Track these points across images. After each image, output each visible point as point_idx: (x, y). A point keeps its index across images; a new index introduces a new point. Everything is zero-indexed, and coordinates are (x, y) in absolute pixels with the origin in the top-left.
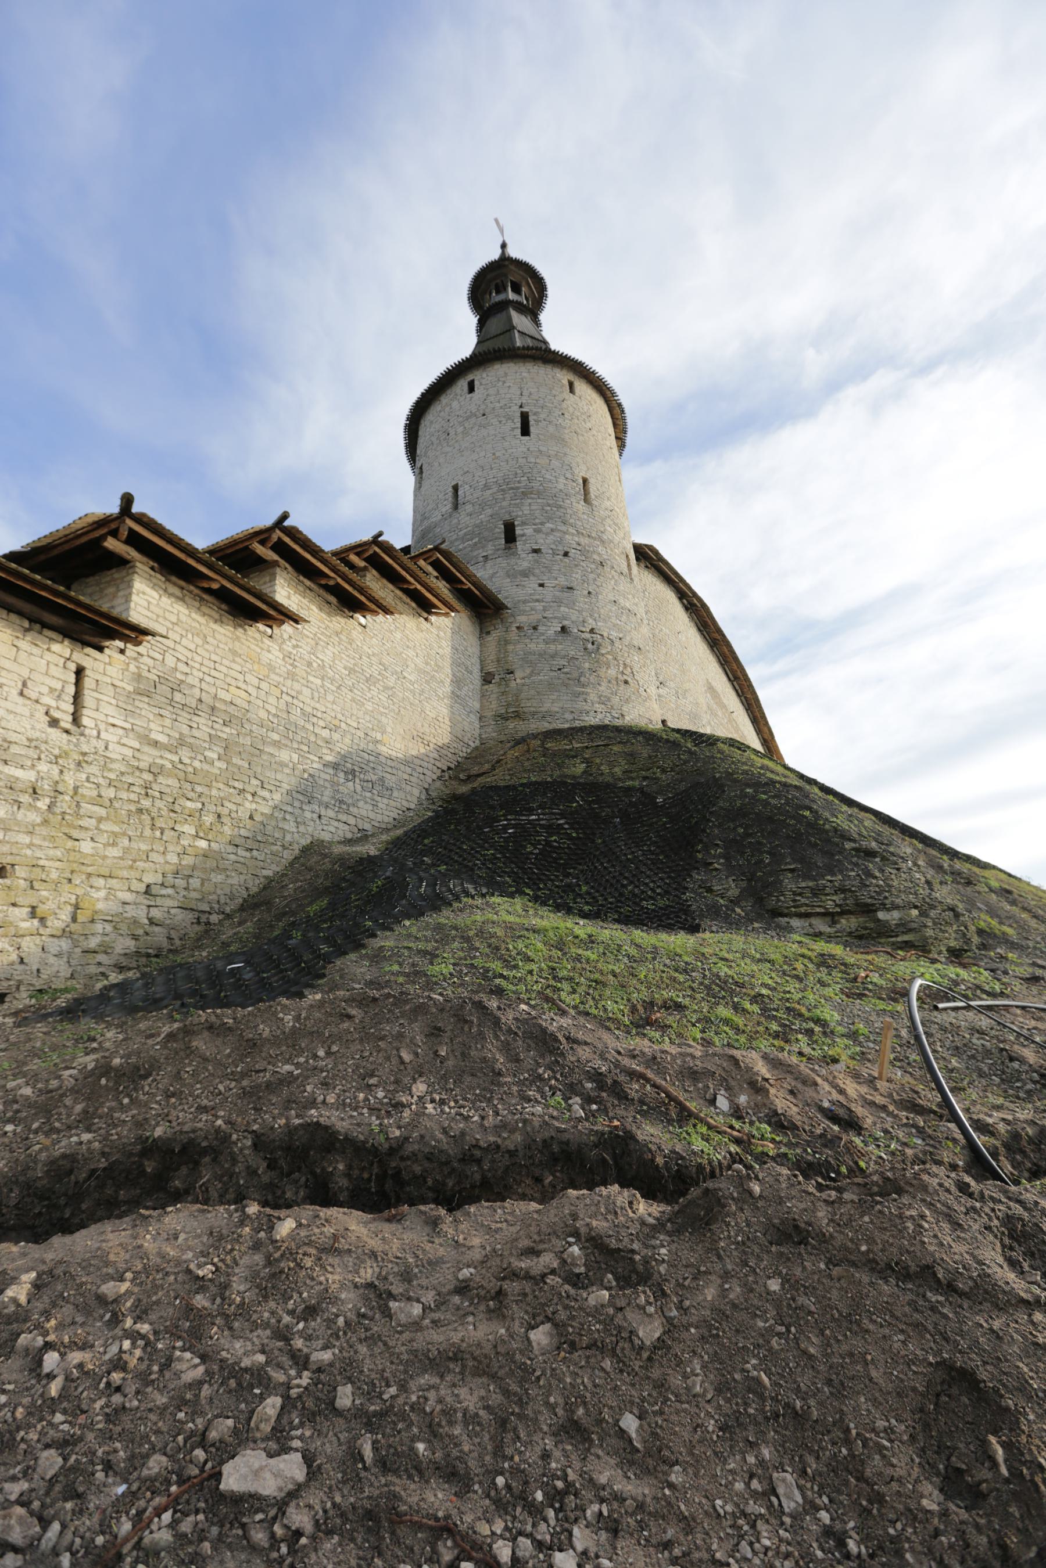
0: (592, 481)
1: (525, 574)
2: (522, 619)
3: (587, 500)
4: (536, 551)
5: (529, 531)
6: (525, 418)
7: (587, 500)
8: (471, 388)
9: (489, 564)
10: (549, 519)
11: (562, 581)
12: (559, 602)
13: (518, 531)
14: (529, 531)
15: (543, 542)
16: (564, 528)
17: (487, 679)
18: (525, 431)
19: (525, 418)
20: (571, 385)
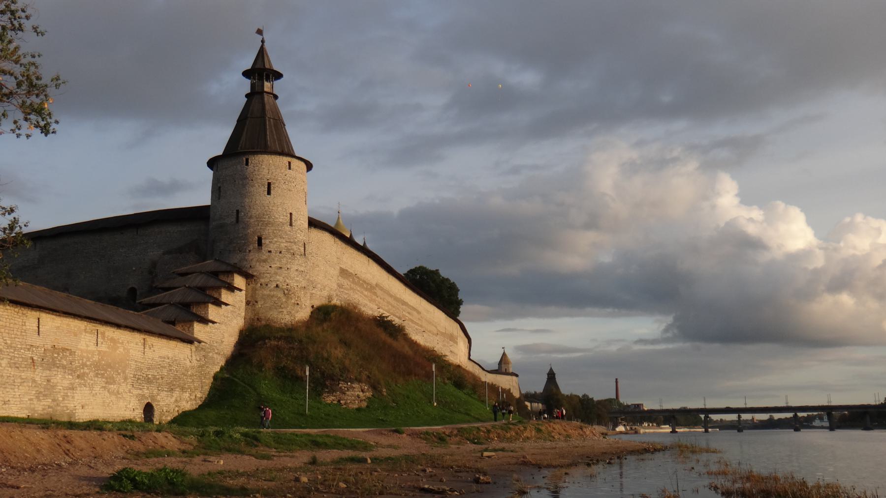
0: (293, 213)
1: (265, 261)
2: (262, 281)
3: (291, 225)
4: (270, 252)
5: (267, 242)
6: (269, 184)
7: (291, 225)
8: (247, 164)
9: (251, 254)
10: (275, 237)
11: (278, 265)
12: (276, 274)
13: (263, 241)
14: (267, 242)
15: (272, 247)
16: (280, 240)
17: (248, 303)
18: (269, 193)
19: (269, 184)
20: (290, 163)
